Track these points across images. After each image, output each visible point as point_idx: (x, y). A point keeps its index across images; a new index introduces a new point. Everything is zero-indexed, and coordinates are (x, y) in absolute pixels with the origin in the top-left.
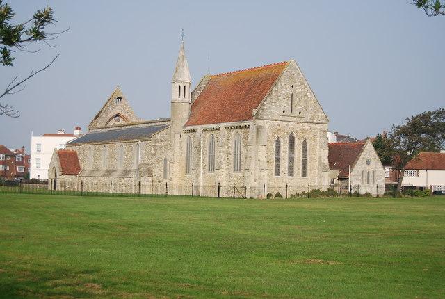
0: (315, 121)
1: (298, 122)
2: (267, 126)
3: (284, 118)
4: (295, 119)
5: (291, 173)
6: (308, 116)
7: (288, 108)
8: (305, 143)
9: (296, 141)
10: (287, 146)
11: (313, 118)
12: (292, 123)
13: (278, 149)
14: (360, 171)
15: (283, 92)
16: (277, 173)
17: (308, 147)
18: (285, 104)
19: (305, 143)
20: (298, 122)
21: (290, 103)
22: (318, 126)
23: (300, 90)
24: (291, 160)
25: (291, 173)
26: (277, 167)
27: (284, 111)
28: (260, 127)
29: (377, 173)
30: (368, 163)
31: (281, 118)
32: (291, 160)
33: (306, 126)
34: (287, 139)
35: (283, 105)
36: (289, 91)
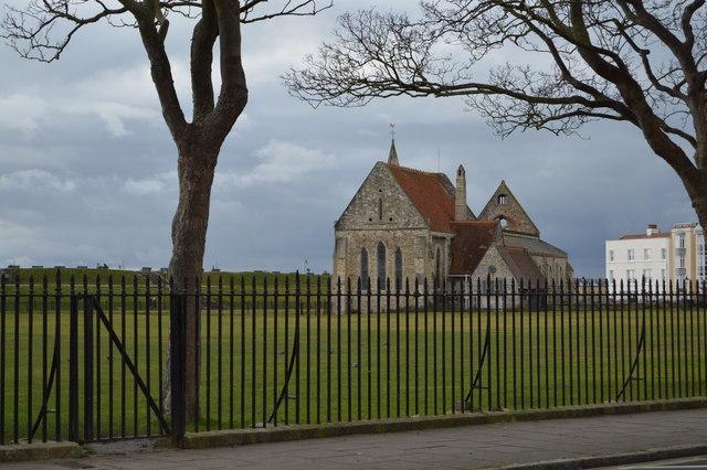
1: (388, 230)
4: (384, 227)
6: (401, 222)
7: (375, 216)
8: (398, 252)
10: (375, 257)
11: (408, 223)
13: (365, 261)
17: (404, 256)
18: (372, 212)
19: (398, 252)
20: (388, 230)
22: (415, 233)
28: (341, 239)
33: (399, 233)
35: (369, 212)
36: (376, 197)
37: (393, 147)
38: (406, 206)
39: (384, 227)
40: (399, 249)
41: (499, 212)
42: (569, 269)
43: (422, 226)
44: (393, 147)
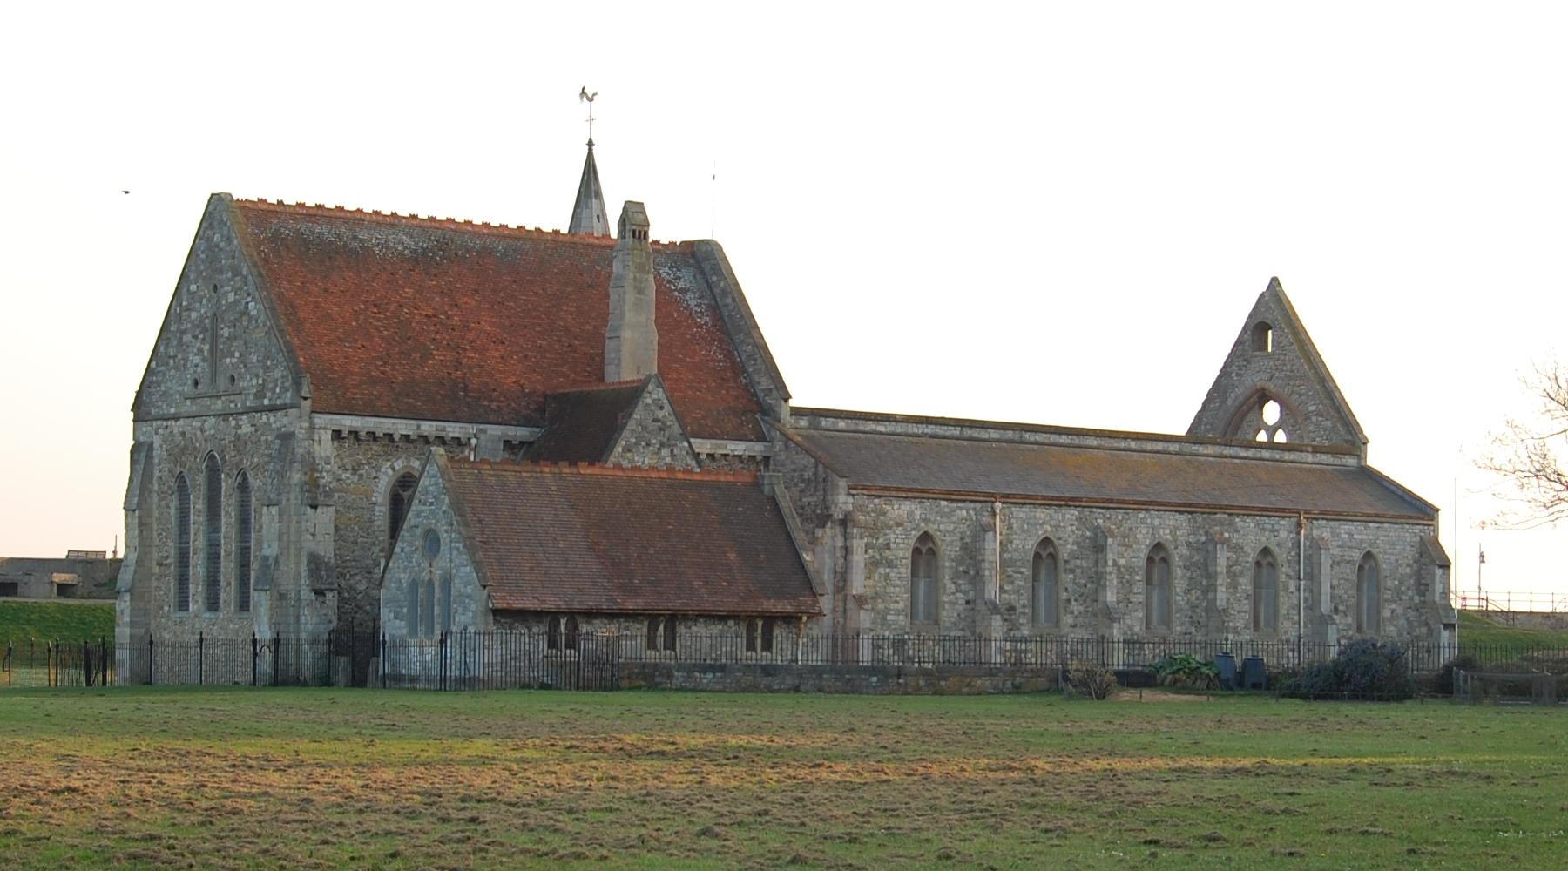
0: (266, 402)
1: (225, 416)
2: (157, 441)
3: (189, 408)
4: (219, 405)
5: (213, 604)
8: (244, 487)
9: (227, 484)
11: (260, 395)
12: (213, 420)
14: (404, 577)
15: (194, 315)
16: (183, 604)
20: (225, 416)
21: (206, 347)
22: (278, 421)
23: (231, 297)
24: (214, 558)
25: (213, 604)
26: (183, 581)
27: (196, 383)
29: (457, 585)
30: (432, 542)
31: (189, 408)
32: (214, 558)
34: (201, 479)
37: (590, 171)
38: (259, 335)
39: (219, 405)
40: (245, 478)
41: (1254, 378)
42: (1433, 560)
43: (288, 398)
44: (590, 171)
